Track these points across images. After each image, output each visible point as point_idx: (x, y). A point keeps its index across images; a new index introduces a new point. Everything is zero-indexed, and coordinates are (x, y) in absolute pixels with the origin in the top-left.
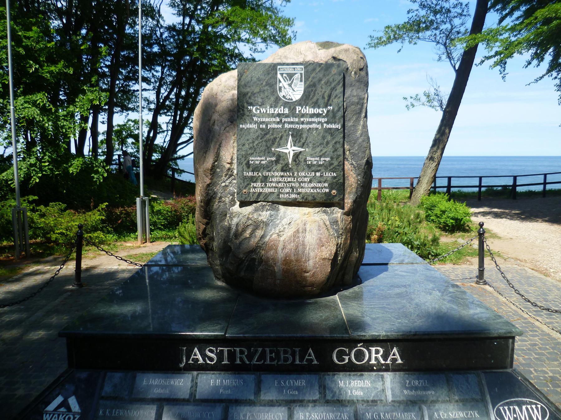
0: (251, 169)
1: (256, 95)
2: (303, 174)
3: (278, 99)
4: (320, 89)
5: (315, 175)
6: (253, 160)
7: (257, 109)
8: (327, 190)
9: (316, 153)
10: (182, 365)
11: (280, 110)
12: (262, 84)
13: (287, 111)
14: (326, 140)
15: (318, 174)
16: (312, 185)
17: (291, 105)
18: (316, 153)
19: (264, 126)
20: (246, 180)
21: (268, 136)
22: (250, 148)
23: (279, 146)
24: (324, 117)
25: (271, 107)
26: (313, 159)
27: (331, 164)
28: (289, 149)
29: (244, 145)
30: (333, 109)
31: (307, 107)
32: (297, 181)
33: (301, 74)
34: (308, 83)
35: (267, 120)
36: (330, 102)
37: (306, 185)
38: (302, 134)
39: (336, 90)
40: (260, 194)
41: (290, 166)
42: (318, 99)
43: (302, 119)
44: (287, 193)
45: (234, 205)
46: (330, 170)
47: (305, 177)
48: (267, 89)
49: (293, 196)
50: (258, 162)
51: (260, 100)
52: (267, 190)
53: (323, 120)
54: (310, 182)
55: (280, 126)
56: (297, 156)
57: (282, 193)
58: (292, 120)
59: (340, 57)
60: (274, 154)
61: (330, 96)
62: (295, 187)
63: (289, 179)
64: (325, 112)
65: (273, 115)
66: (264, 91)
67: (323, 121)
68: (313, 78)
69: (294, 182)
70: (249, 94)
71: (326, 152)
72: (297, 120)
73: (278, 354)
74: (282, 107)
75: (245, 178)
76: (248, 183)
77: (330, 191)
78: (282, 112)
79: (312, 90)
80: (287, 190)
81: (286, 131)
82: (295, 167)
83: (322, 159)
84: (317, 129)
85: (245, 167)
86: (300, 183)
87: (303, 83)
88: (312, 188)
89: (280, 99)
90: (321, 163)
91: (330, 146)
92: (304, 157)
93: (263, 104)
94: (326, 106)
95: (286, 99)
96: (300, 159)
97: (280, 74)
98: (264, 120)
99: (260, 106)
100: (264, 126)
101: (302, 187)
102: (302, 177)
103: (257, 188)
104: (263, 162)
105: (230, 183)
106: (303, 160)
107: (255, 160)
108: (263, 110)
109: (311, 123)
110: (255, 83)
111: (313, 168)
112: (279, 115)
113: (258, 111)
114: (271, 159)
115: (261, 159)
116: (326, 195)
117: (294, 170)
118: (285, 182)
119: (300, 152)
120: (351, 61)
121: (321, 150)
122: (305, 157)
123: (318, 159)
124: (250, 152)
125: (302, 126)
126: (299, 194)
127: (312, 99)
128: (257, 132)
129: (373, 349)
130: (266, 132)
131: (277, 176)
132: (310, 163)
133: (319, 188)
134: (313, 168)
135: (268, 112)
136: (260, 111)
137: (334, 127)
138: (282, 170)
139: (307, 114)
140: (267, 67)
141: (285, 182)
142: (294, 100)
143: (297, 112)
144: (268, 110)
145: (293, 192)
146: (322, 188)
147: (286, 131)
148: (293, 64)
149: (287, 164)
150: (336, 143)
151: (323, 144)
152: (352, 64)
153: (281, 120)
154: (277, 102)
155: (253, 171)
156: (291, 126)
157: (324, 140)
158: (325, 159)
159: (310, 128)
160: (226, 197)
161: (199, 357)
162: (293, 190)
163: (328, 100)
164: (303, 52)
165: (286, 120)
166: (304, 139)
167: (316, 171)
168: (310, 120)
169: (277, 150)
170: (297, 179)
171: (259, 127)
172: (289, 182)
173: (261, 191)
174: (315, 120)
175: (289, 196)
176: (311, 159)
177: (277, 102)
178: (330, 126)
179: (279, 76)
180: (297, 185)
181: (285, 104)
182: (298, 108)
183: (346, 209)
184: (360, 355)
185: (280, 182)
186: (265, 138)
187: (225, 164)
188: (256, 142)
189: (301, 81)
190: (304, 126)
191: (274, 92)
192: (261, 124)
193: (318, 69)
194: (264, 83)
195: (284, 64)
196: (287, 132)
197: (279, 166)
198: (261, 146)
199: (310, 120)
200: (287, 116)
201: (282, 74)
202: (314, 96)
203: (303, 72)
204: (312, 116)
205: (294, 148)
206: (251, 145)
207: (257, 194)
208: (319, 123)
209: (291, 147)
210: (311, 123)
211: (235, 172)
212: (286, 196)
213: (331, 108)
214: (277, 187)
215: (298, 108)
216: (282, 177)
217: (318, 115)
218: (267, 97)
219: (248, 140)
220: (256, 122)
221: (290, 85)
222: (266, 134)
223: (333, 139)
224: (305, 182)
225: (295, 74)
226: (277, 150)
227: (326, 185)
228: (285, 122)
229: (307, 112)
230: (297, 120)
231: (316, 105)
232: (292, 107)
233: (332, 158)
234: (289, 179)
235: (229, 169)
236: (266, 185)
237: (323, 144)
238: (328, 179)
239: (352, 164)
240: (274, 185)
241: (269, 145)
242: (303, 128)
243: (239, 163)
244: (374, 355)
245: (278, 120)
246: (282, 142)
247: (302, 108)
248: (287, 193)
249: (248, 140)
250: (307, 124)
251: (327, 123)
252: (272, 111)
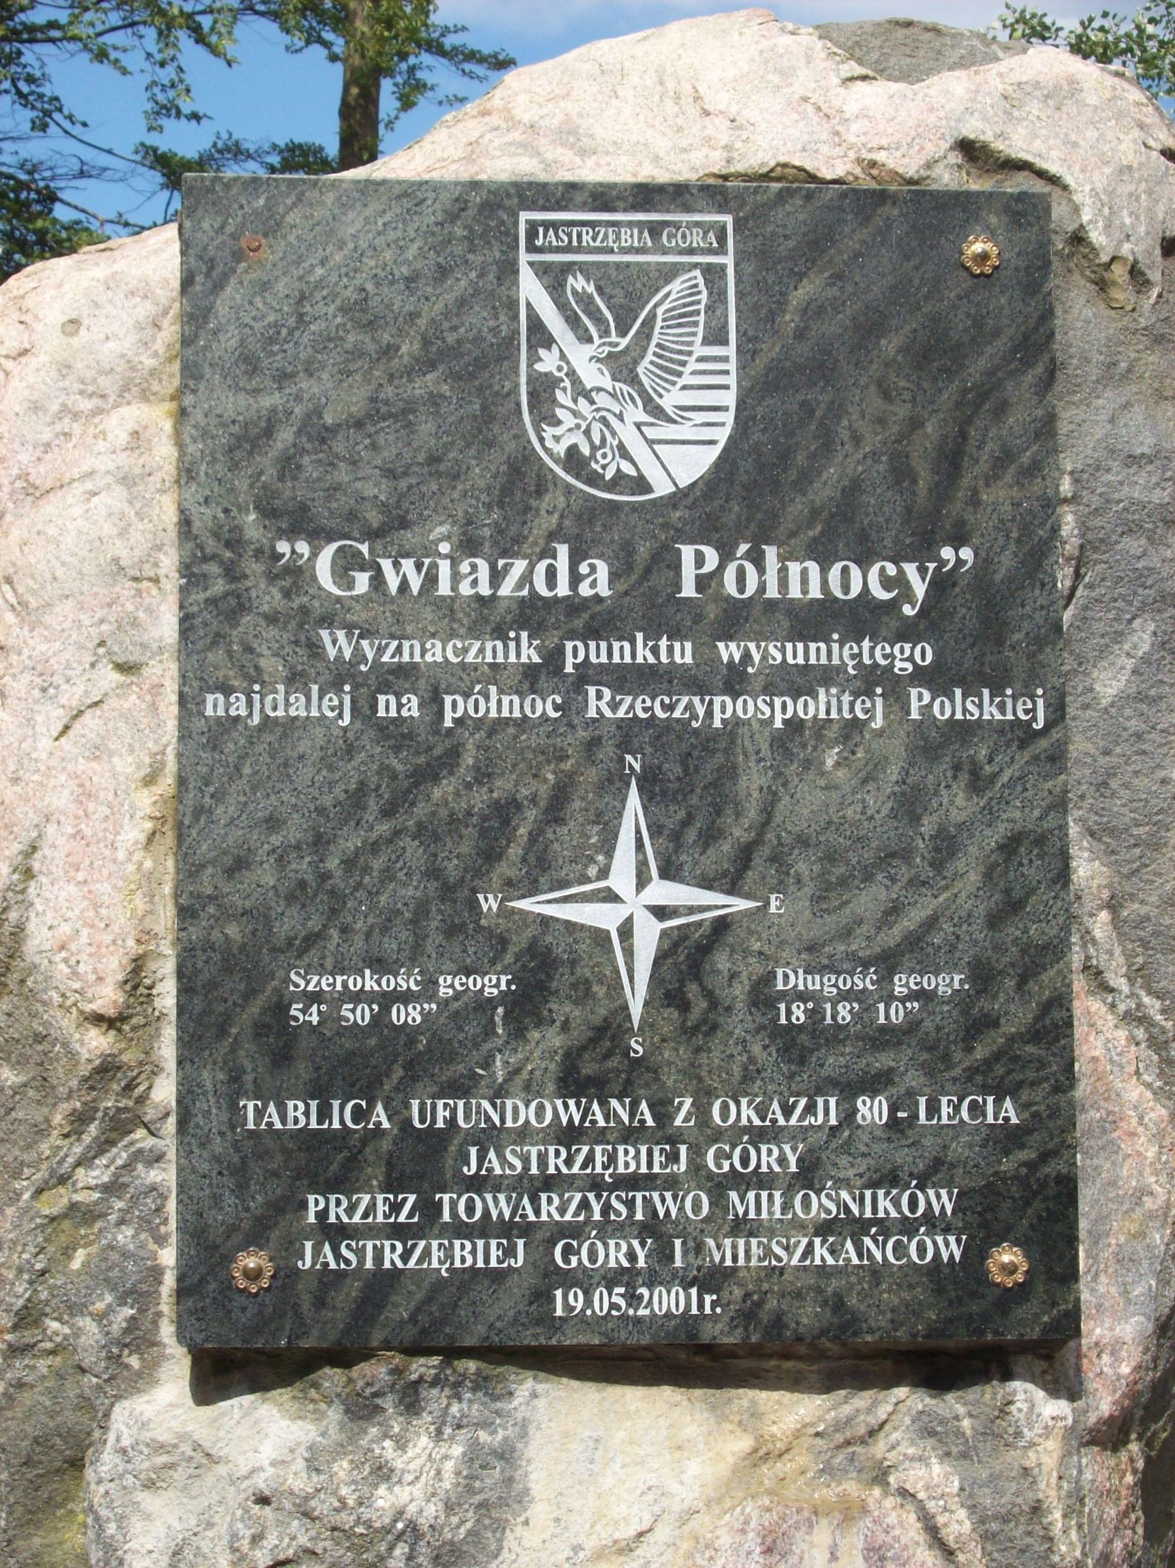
0: (303, 1070)
1: (339, 446)
2: (748, 1114)
3: (522, 479)
4: (875, 403)
5: (848, 1116)
6: (316, 997)
7: (346, 565)
8: (951, 1248)
9: (847, 933)
11: (554, 575)
12: (389, 351)
13: (599, 580)
14: (928, 826)
15: (872, 1110)
16: (822, 1205)
17: (635, 530)
18: (847, 933)
19: (412, 707)
20: (256, 1170)
21: (443, 790)
22: (298, 894)
23: (539, 873)
24: (908, 633)
25: (468, 546)
26: (826, 984)
27: (979, 1026)
28: (628, 902)
29: (239, 865)
30: (984, 562)
31: (771, 553)
32: (697, 1167)
33: (713, 274)
34: (771, 349)
35: (437, 652)
36: (956, 507)
37: (767, 1206)
38: (730, 772)
39: (1002, 409)
40: (385, 1281)
41: (637, 1047)
42: (853, 489)
43: (729, 651)
44: (612, 1278)
45: (143, 1380)
46: (971, 1073)
47: (759, 1136)
48: (435, 399)
49: (668, 1301)
50: (361, 1015)
51: (375, 488)
52: (438, 1257)
53: (905, 657)
54: (809, 1175)
55: (545, 707)
56: (689, 955)
57: (569, 1280)
58: (644, 655)
59: (1017, 145)
61: (951, 459)
62: (682, 1227)
63: (629, 1160)
64: (920, 589)
65: (487, 618)
66: (409, 408)
67: (902, 666)
68: (813, 311)
69: (671, 1183)
70: (285, 436)
71: (931, 923)
72: (684, 654)
74: (563, 550)
76: (277, 1189)
77: (976, 1254)
78: (563, 590)
79: (807, 409)
80: (614, 1254)
81: (593, 744)
82: (674, 1056)
83: (901, 984)
84: (854, 727)
85: (250, 1058)
86: (718, 1187)
87: (731, 351)
88: (824, 1229)
89: (543, 483)
90: (897, 1014)
91: (968, 871)
92: (752, 968)
93: (404, 524)
94: (922, 548)
95: (594, 479)
96: (716, 983)
97: (542, 270)
98: (411, 651)
99: (372, 535)
100: (412, 707)
101: (741, 1227)
102: (737, 1133)
103: (361, 1232)
104: (408, 1015)
105: (112, 1188)
106: (740, 991)
107: (331, 992)
109: (799, 681)
110: (326, 342)
111: (834, 1062)
112: (532, 614)
113: (362, 582)
114: (475, 983)
115: (389, 983)
116: (939, 1291)
117: (670, 1079)
118: (596, 1185)
119: (722, 925)
120: (1101, 178)
121: (894, 911)
122: (757, 968)
123: (865, 982)
124: (290, 922)
125: (724, 708)
126: (711, 1279)
127: (805, 479)
128: (350, 750)
130: (428, 755)
131: (524, 1134)
132: (799, 1014)
133: (884, 1227)
134: (834, 1062)
135: (444, 588)
136: (378, 580)
137: (991, 712)
138: (573, 1082)
139: (771, 603)
140: (430, 216)
141: (596, 1185)
142: (662, 488)
143: (688, 590)
144: (444, 567)
145: (659, 1274)
146: (908, 1227)
147: (593, 744)
148: (645, 195)
149: (611, 1030)
150: (1010, 846)
151: (905, 854)
152: (1108, 202)
153: (554, 658)
154: (517, 502)
155: (320, 1092)
156: (635, 706)
157: (916, 820)
158: (929, 982)
159: (794, 725)
160: (74, 1309)
162: (664, 1254)
163: (943, 492)
164: (718, 100)
165: (598, 653)
166: (752, 813)
167: (850, 1089)
168: (796, 654)
169: (524, 904)
170: (697, 1152)
171: (364, 710)
172: (632, 1182)
173: (392, 1257)
174: (840, 653)
175: (633, 1299)
176: (814, 983)
177: (517, 502)
178: (955, 707)
179: (530, 289)
180: (694, 1204)
181: (587, 529)
182: (693, 561)
183: (1104, 1403)
185: (549, 1183)
186: (421, 810)
187: (66, 1023)
188: (351, 841)
189: (716, 336)
190: (747, 708)
191: (490, 418)
192: (385, 687)
193: (853, 237)
194: (408, 348)
195: (566, 194)
196: (608, 751)
197: (546, 1044)
198: (388, 875)
199: (796, 654)
200: (597, 621)
201: (554, 279)
202: (828, 445)
203: (729, 260)
204: (812, 620)
205: (662, 892)
206: (302, 866)
207: (354, 1289)
208: (871, 679)
209: (642, 881)
210: (799, 681)
211: (165, 1091)
212: (605, 1301)
213: (966, 553)
214: (526, 1229)
215: (693, 561)
216: (569, 1136)
217: (861, 619)
218: (434, 460)
219: (273, 823)
220: (341, 675)
221: (622, 367)
222: (427, 774)
223: (990, 813)
224: (762, 1181)
225: (670, 273)
226: (524, 904)
227: (942, 1201)
228: (586, 674)
229: (772, 592)
230: (684, 654)
231: (840, 534)
232: (643, 550)
233: (983, 976)
234: (629, 1160)
235: (107, 1069)
236: (429, 1209)
237: (905, 854)
238: (958, 1149)
239: (1135, 1017)
240: (501, 1207)
241: (452, 868)
242: (734, 725)
245: (530, 654)
246: (563, 840)
247: (726, 556)
248: (612, 1278)
249: (273, 823)
250: (770, 689)
251: (936, 678)
252: (475, 577)
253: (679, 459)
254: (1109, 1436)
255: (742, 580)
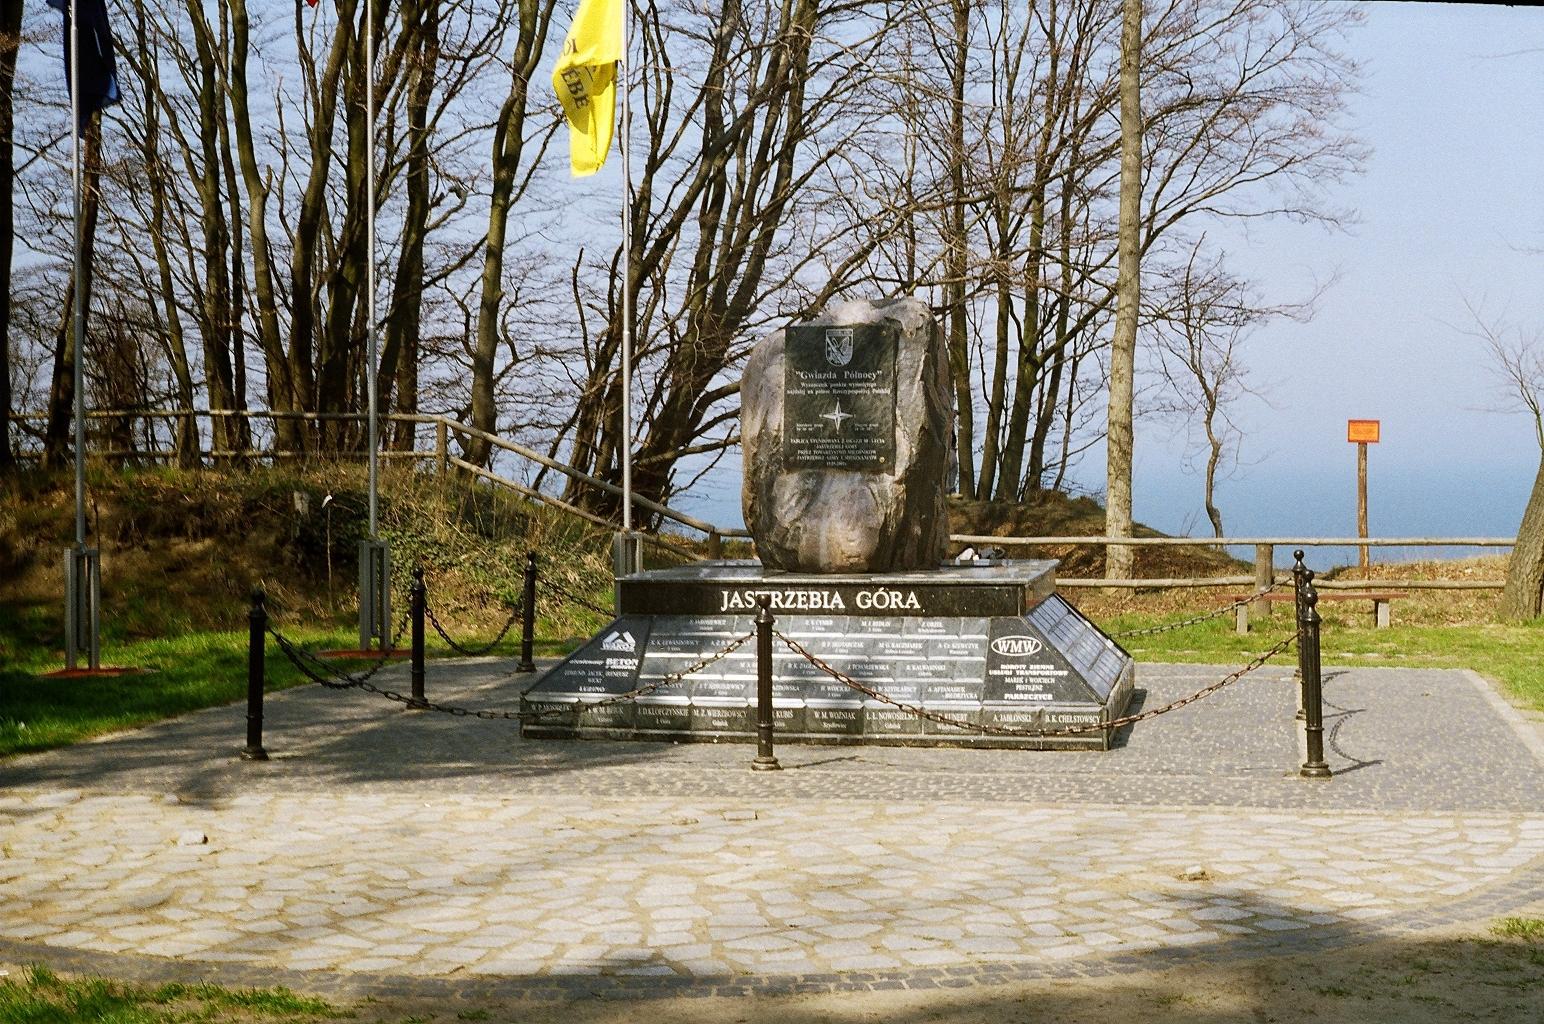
10: (723, 609)
11: (830, 375)
17: (839, 370)
23: (826, 412)
56: (844, 422)
60: (821, 421)
73: (808, 597)
75: (792, 445)
108: (811, 376)
112: (827, 380)
129: (893, 594)
154: (825, 367)
161: (739, 601)
177: (825, 367)
181: (833, 370)
184: (881, 599)
191: (822, 355)
200: (835, 381)
243: (786, 431)
244: (894, 600)
253: (845, 360)
254: (899, 482)
255: (852, 376)
